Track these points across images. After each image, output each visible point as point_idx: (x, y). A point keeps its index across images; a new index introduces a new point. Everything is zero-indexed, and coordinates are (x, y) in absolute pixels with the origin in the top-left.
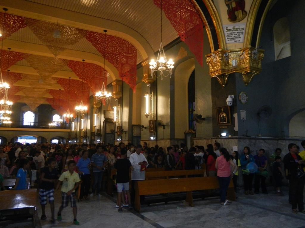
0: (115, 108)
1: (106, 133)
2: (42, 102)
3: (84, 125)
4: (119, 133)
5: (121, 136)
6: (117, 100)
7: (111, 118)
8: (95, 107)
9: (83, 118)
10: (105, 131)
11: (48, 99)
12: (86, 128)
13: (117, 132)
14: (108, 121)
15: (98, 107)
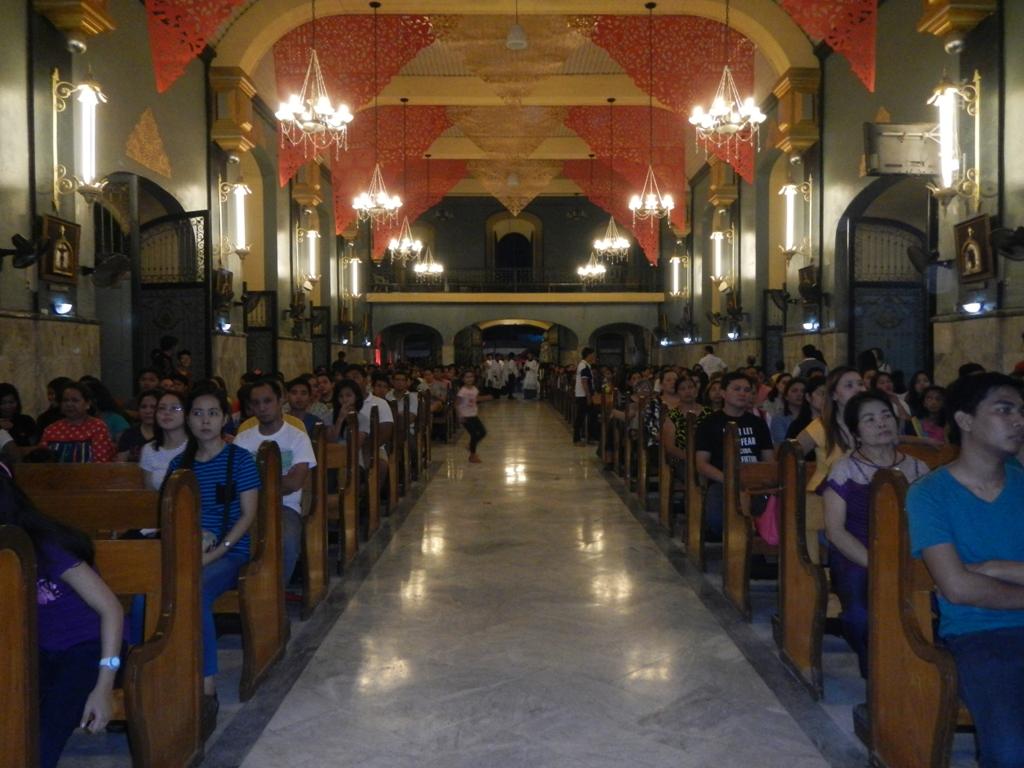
0: (946, 101)
1: (854, 287)
2: (548, 185)
3: (733, 259)
4: (974, 266)
5: (993, 283)
6: (955, 47)
7: (916, 170)
8: (787, 147)
9: (719, 230)
10: (852, 271)
11: (568, 169)
12: (735, 275)
13: (949, 264)
14: (893, 203)
15: (805, 144)
